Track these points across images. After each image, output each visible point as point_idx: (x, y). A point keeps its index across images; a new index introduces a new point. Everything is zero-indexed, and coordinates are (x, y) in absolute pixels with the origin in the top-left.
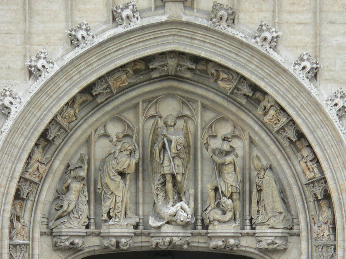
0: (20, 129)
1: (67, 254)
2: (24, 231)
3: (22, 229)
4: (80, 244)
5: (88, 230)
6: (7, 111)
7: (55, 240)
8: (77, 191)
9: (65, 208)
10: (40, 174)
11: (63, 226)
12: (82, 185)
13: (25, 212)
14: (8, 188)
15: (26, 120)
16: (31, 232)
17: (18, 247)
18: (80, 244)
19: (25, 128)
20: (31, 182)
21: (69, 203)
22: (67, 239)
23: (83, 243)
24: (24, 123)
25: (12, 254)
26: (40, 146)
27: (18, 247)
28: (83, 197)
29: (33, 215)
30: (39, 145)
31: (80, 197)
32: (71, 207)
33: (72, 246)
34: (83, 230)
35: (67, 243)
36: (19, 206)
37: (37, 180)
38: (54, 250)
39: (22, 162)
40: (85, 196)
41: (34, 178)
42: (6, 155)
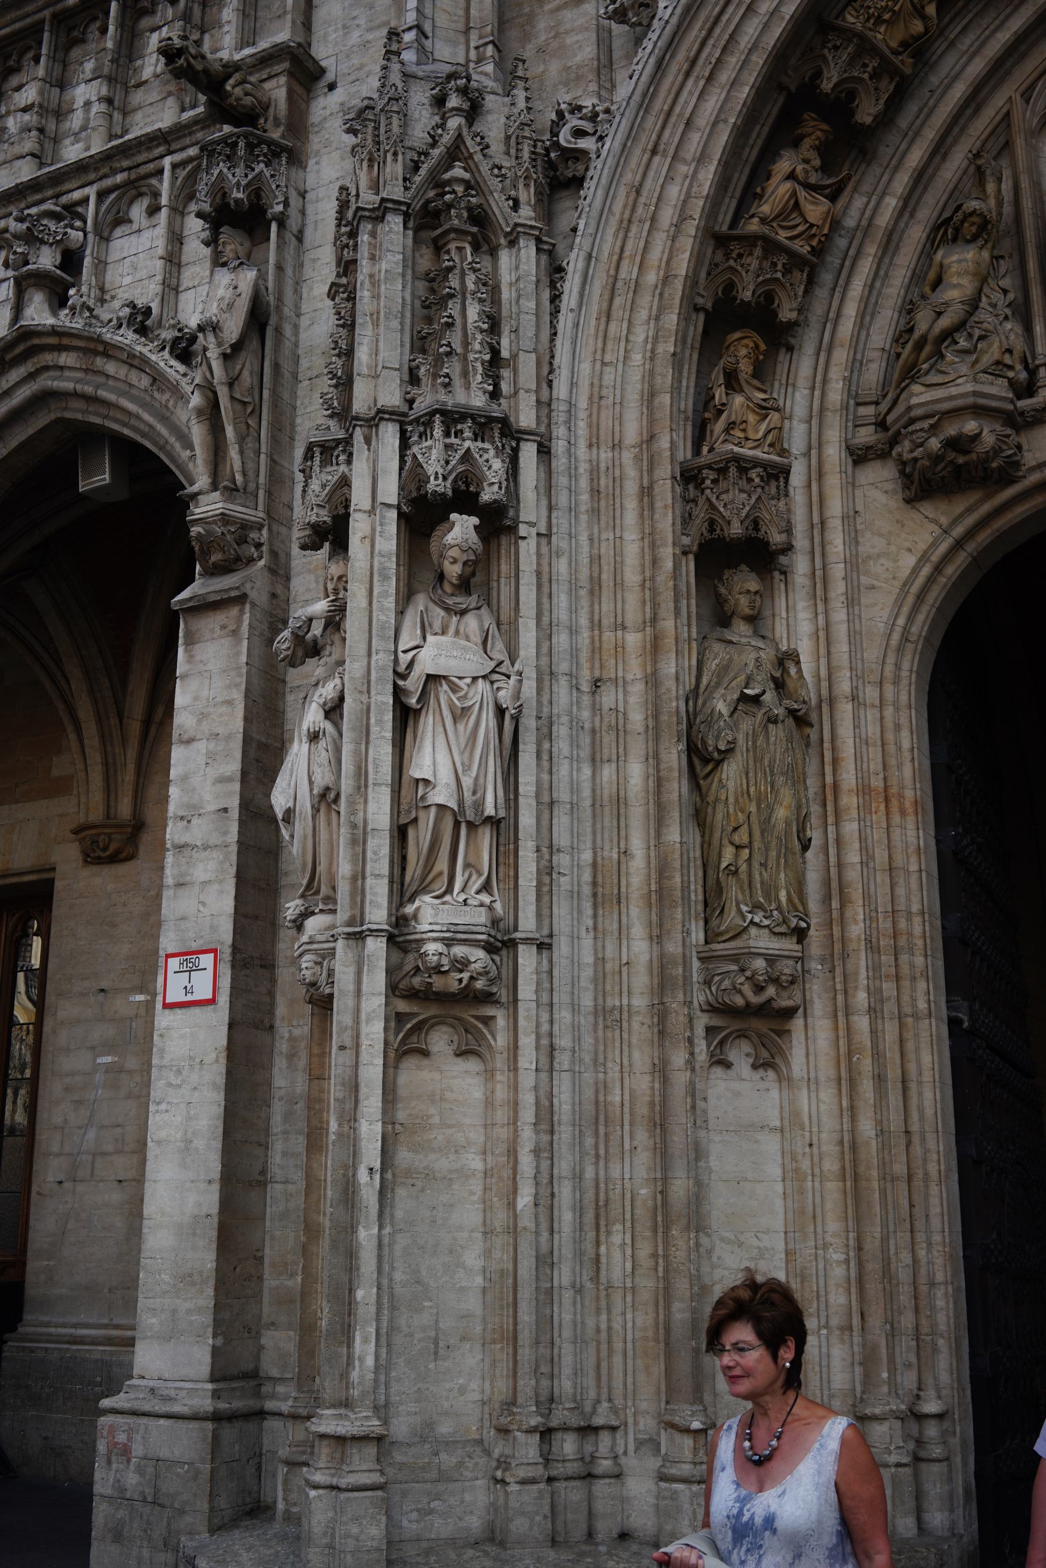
0: (701, 61)
1: (959, 506)
2: (763, 427)
3: (752, 418)
4: (988, 439)
5: (1023, 404)
6: (645, 13)
7: (898, 449)
8: (967, 272)
9: (921, 328)
10: (812, 226)
11: (916, 388)
12: (986, 254)
13: (790, 389)
14: (668, 263)
15: (717, 31)
16: (815, 447)
17: (733, 471)
18: (988, 439)
19: (717, 55)
20: (771, 247)
21: (939, 314)
22: (934, 429)
23: (1002, 439)
24: (711, 42)
25: (714, 500)
26: (807, 142)
27: (733, 471)
28: (997, 297)
29: (817, 393)
30: (802, 137)
31: (984, 299)
32: (944, 322)
33: (961, 460)
34: (999, 388)
35: (934, 444)
36: (744, 352)
37: (802, 248)
38: (908, 501)
39: (710, 163)
40: (1005, 292)
41: (786, 238)
42: (657, 159)
